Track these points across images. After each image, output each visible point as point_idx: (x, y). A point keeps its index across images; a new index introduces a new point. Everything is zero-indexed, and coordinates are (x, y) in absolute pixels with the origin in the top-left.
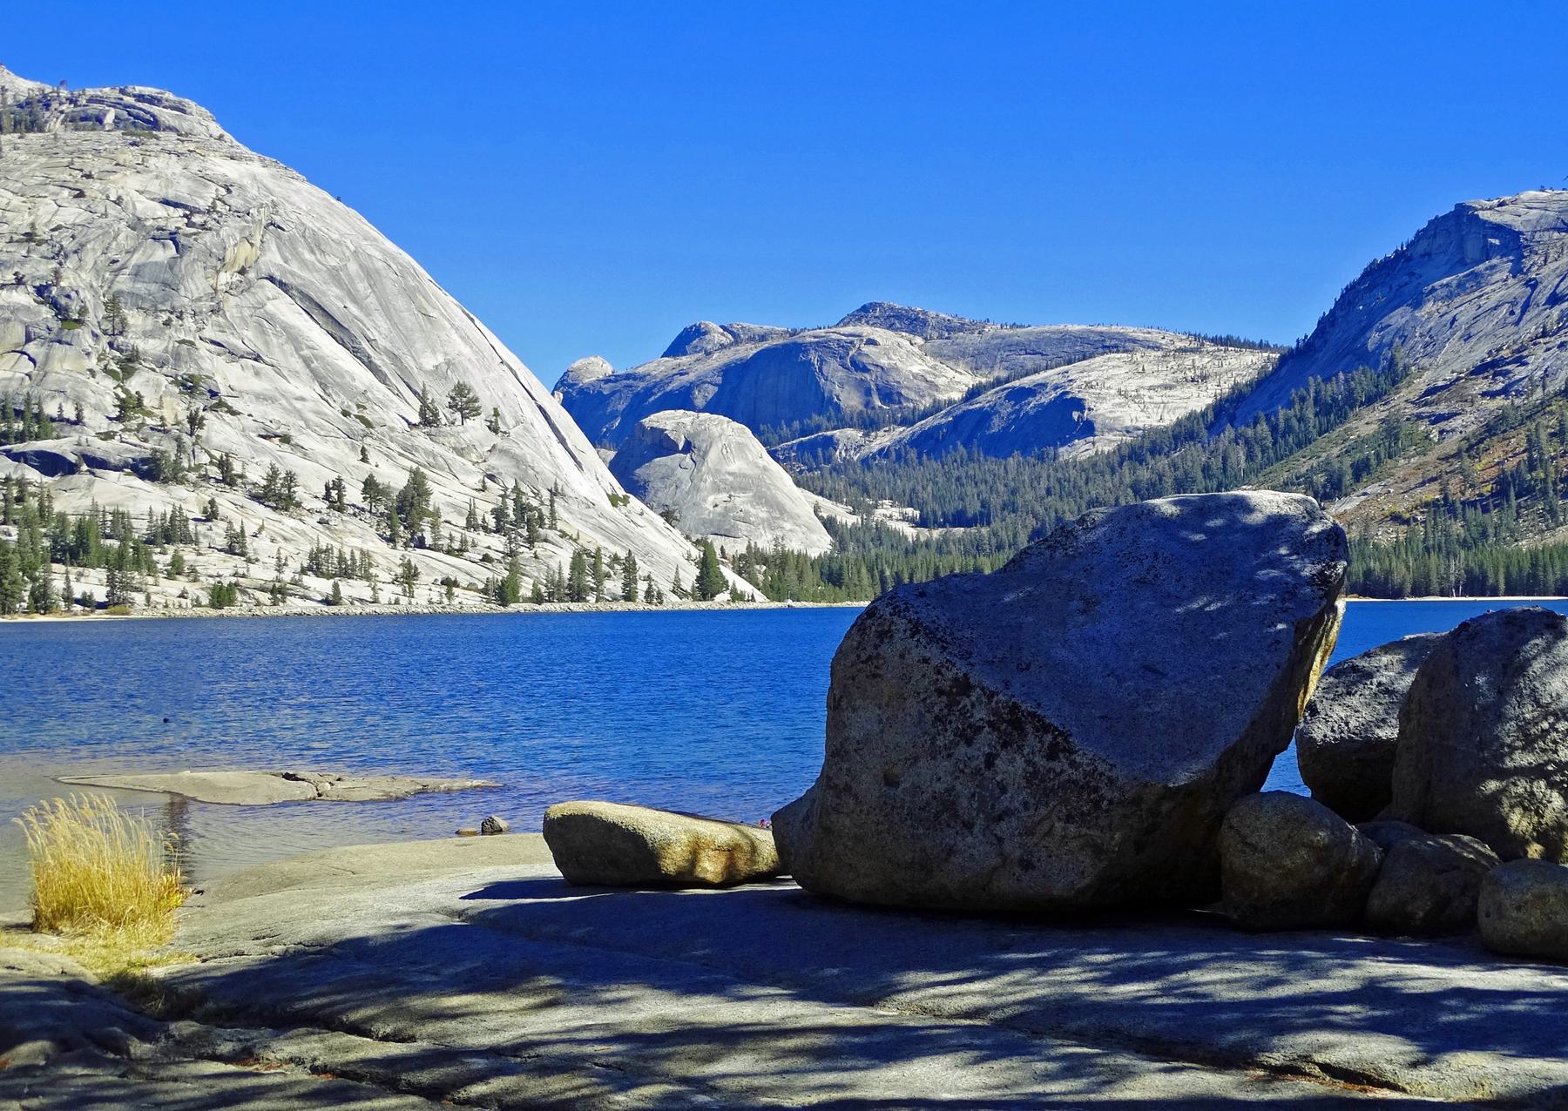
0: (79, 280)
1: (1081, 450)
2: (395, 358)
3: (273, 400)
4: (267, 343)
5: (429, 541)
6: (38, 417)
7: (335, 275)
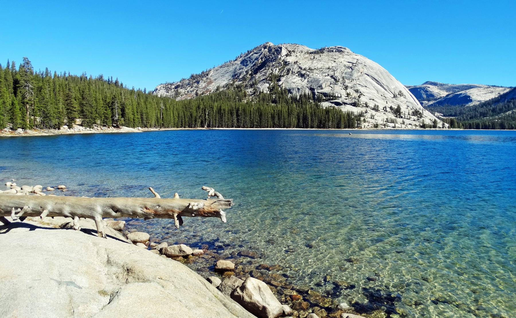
0: (337, 75)
1: (471, 104)
2: (387, 86)
3: (370, 93)
6: (335, 96)
7: (376, 73)
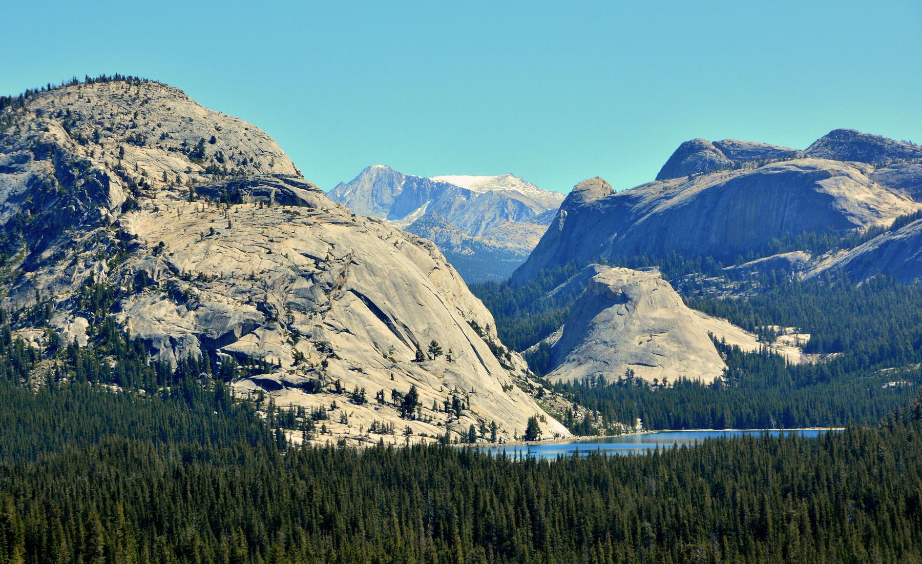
4: (351, 323)
5: (417, 417)
7: (380, 287)
